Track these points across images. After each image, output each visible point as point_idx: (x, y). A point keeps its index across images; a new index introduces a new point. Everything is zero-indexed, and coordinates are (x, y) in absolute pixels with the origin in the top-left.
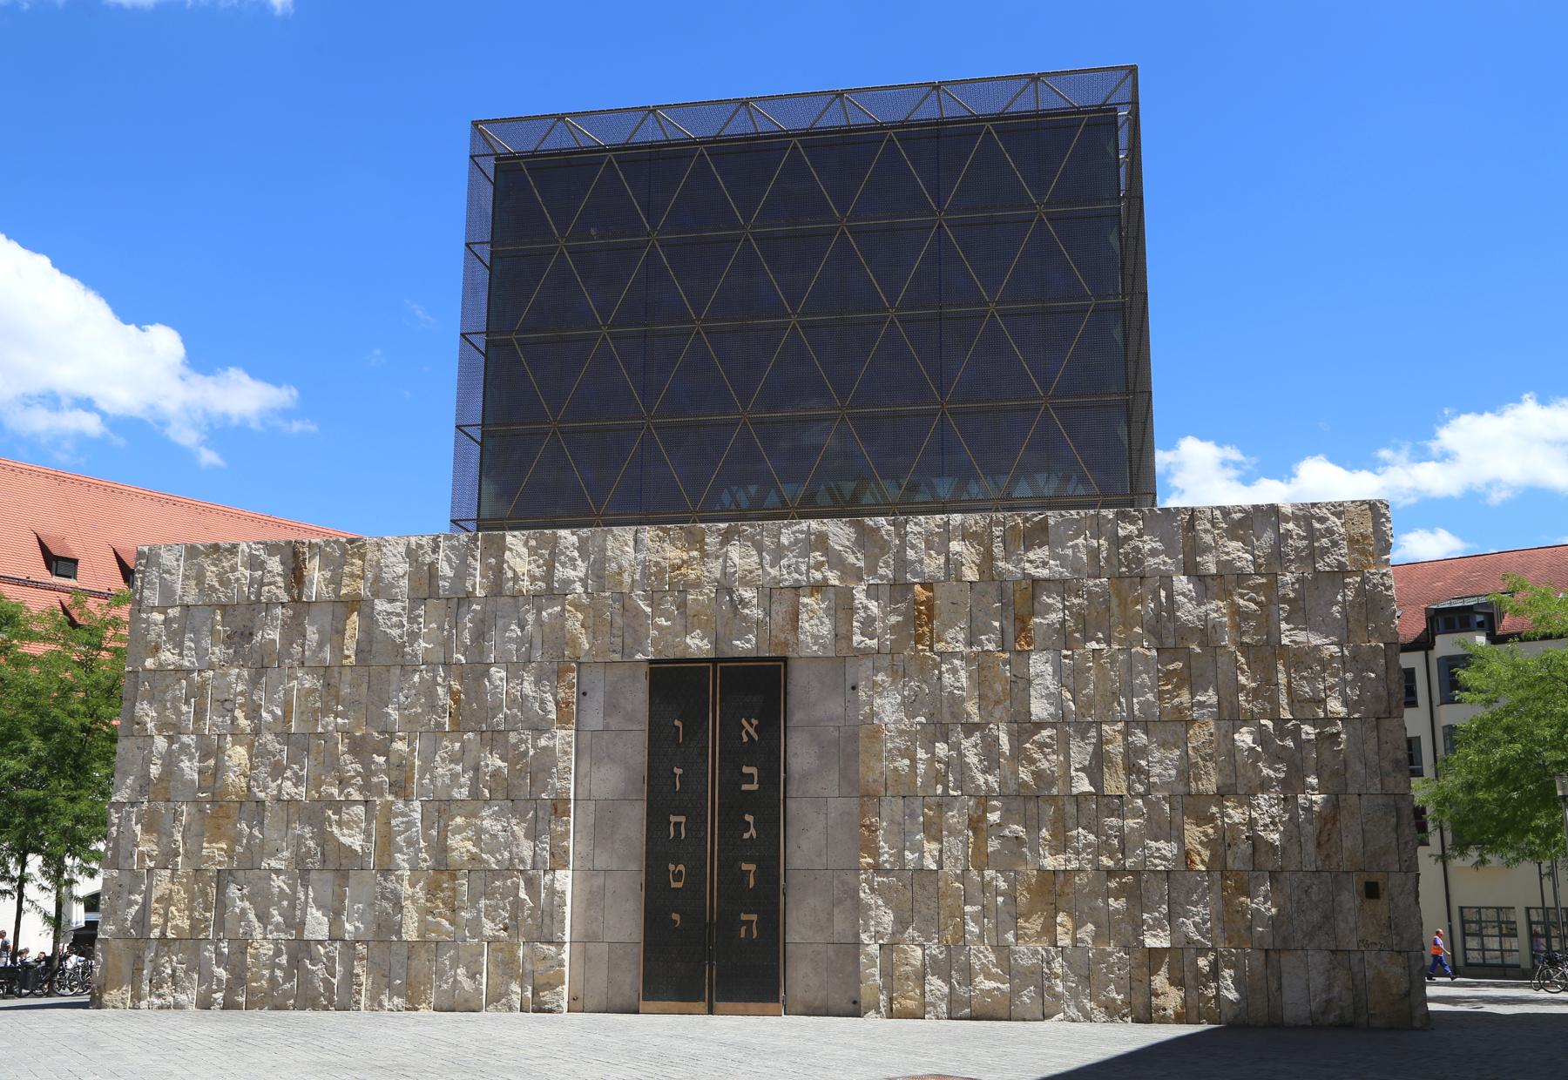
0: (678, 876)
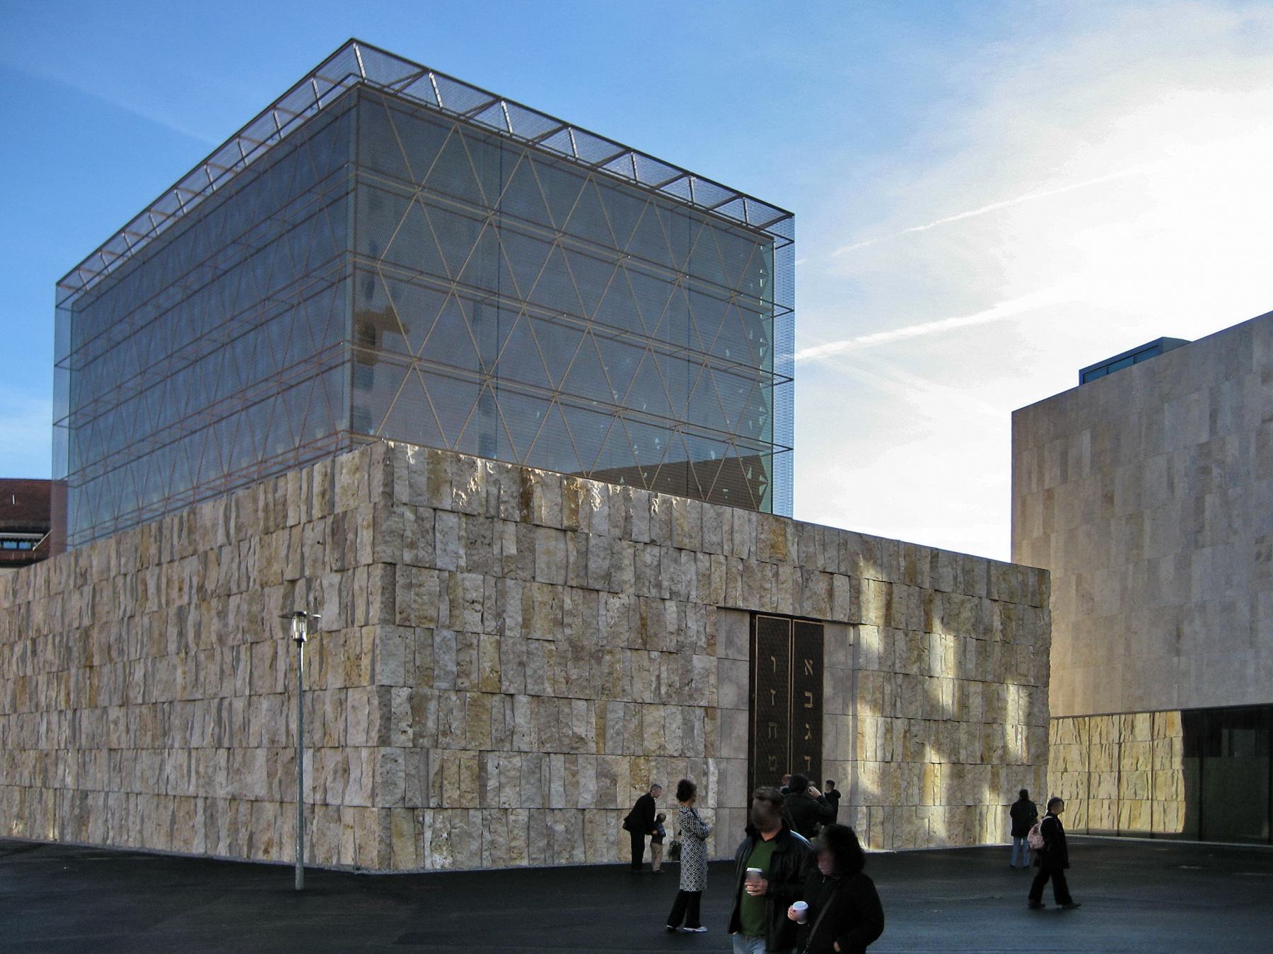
0: (773, 765)
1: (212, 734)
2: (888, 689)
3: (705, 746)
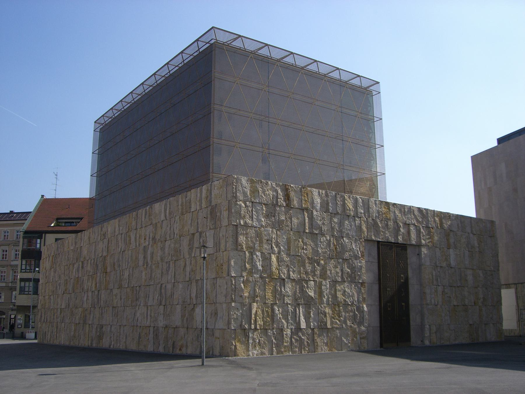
1: (157, 299)
2: (434, 274)
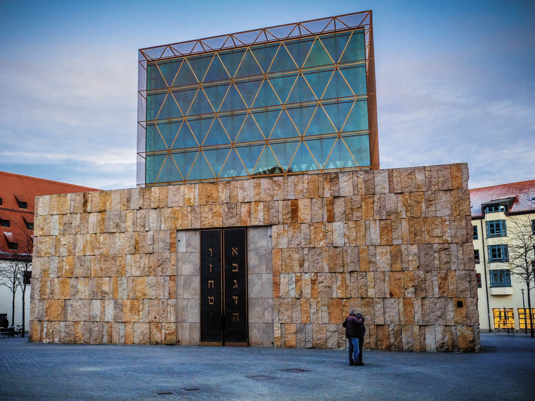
3: (170, 294)
